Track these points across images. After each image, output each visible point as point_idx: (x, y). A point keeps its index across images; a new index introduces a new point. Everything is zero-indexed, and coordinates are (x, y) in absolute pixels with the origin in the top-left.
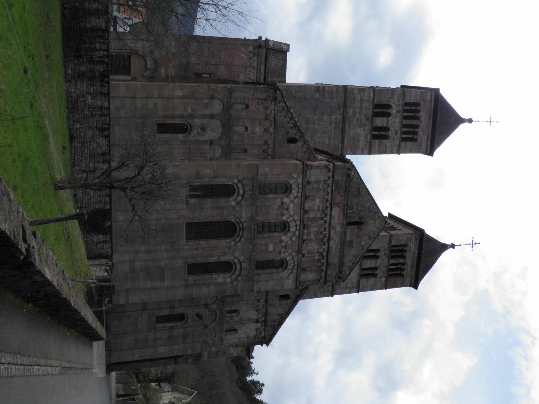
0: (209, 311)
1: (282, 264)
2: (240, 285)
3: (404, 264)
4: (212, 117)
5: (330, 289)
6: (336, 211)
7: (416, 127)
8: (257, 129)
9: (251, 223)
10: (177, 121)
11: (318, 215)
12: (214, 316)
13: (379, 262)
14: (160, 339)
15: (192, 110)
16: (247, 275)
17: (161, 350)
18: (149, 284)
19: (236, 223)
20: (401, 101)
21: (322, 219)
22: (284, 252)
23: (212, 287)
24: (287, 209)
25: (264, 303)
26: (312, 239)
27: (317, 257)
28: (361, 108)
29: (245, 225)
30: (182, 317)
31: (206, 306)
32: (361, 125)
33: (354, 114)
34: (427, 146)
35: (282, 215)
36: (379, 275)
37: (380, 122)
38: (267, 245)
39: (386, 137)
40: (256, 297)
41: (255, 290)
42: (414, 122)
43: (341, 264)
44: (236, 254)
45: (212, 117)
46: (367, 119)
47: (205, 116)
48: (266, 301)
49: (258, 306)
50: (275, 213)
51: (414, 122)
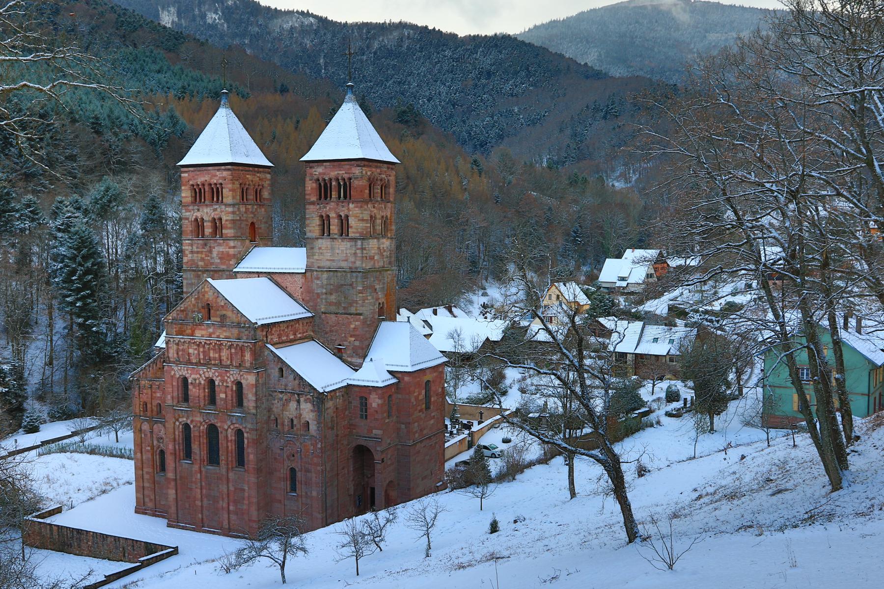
1: (239, 384)
2: (249, 426)
3: (337, 180)
4: (152, 432)
5: (354, 274)
7: (210, 185)
8: (158, 395)
11: (201, 350)
13: (333, 215)
14: (306, 493)
17: (314, 494)
18: (246, 502)
20: (191, 208)
21: (204, 347)
22: (227, 382)
24: (195, 380)
26: (220, 356)
27: (233, 351)
28: (198, 252)
30: (293, 470)
32: (210, 251)
33: (202, 259)
34: (225, 170)
35: (200, 383)
36: (346, 212)
37: (208, 231)
39: (220, 219)
41: (254, 411)
42: (207, 188)
44: (226, 427)
45: (152, 432)
46: (206, 245)
47: (152, 437)
48: (282, 392)
51: (207, 188)
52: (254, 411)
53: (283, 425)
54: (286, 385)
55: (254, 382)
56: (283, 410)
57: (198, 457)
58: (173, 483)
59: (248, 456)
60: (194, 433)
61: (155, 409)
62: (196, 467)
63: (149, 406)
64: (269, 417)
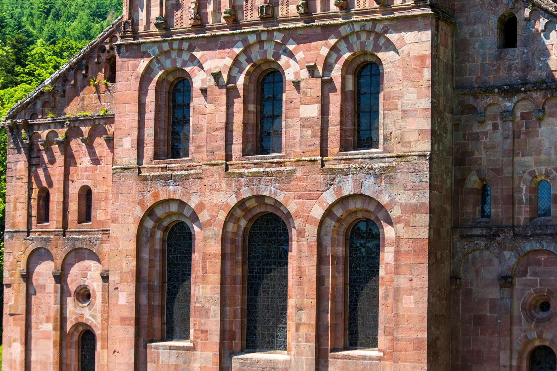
0: (525, 273)
2: (405, 198)
9: (241, 175)
10: (73, 355)
12: (543, 258)
15: (48, 320)
16: (377, 176)
19: (250, 216)
23: (403, 281)
24: (217, 76)
25: (515, 99)
29: (246, 193)
31: (506, 281)
38: (305, 123)
40: (495, 127)
48: (510, 91)
49: (523, 116)
50: (224, 108)
52: (425, 146)
53: (511, 200)
54: (527, 67)
55: (426, 49)
56: (513, 153)
57: (213, 324)
59: (397, 300)
60: (207, 245)
61: (73, 206)
63: (56, 198)
64: (460, 182)
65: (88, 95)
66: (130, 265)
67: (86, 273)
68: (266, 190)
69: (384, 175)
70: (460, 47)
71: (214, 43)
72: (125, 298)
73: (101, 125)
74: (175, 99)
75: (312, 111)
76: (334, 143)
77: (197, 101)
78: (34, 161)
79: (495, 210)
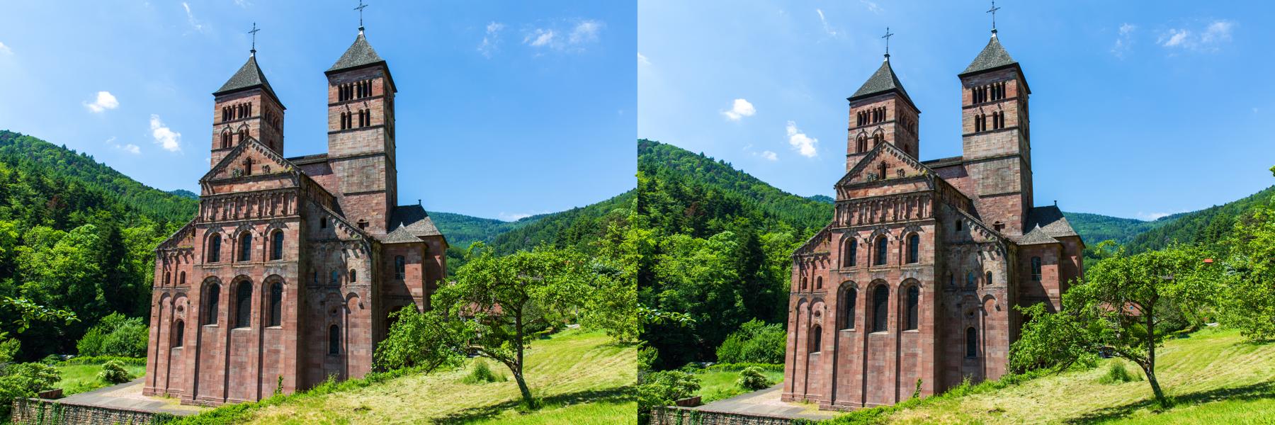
6: (237, 188)
43: (282, 176)
58: (193, 352)
60: (224, 291)
62: (223, 330)
64: (308, 270)
65: (186, 240)
66: (198, 298)
67: (182, 301)
68: (245, 273)
69: (284, 268)
70: (308, 227)
71: (229, 225)
72: (195, 310)
73: (190, 251)
74: (215, 242)
75: (261, 247)
76: (267, 258)
77: (223, 243)
78: (165, 262)
79: (319, 280)
